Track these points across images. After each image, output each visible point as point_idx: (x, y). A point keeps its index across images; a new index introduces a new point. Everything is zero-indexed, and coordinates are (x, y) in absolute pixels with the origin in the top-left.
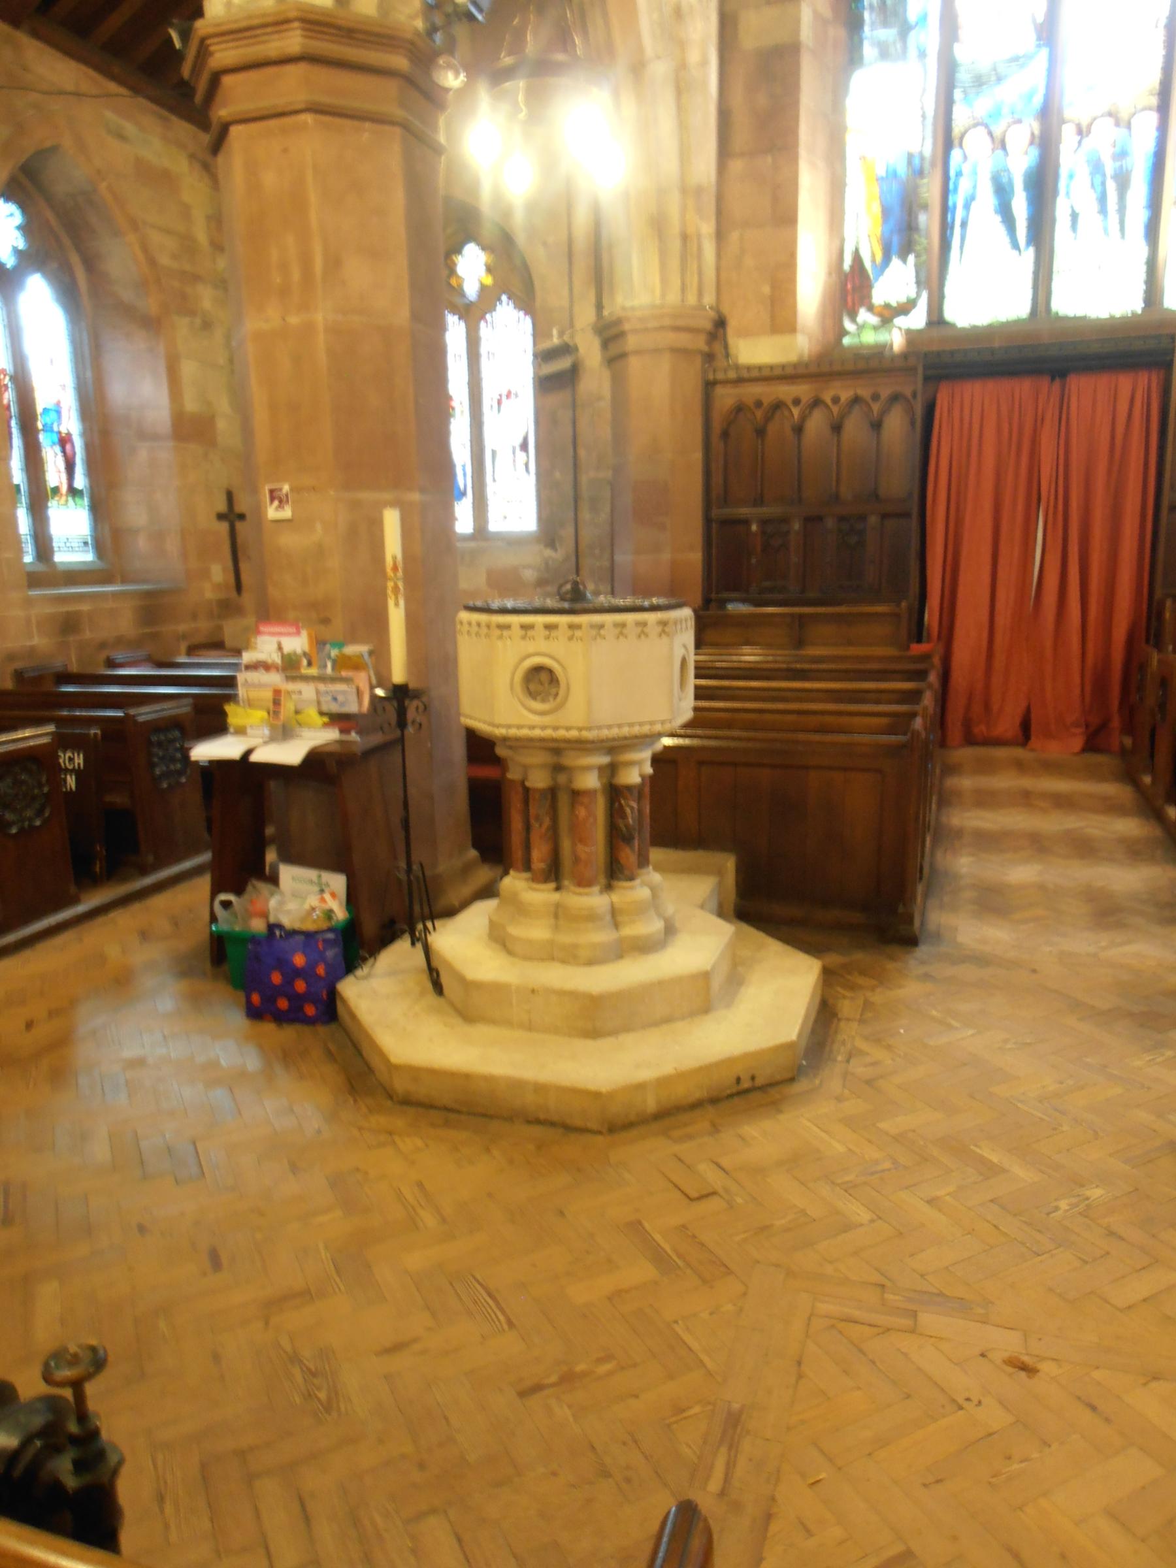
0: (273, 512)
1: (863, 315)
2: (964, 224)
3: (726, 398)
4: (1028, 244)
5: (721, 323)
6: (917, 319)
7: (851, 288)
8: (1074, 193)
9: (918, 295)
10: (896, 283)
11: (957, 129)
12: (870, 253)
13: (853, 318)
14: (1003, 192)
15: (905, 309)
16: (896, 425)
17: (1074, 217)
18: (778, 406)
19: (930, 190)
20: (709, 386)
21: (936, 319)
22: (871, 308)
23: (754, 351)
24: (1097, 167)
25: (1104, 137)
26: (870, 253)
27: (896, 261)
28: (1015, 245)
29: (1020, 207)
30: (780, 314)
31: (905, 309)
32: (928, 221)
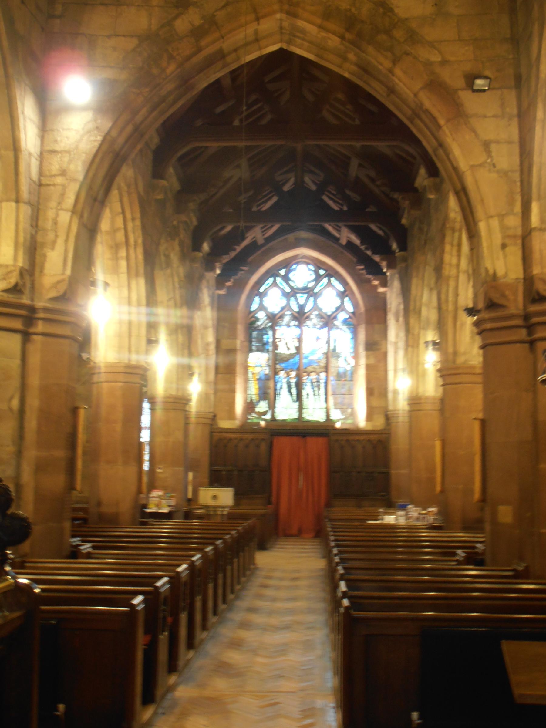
3: (217, 436)
5: (215, 416)
6: (268, 416)
7: (250, 406)
8: (307, 389)
10: (263, 406)
12: (255, 398)
14: (289, 387)
15: (265, 413)
16: (264, 447)
18: (231, 439)
19: (271, 384)
20: (212, 433)
21: (273, 419)
23: (224, 424)
25: (313, 376)
26: (255, 398)
29: (294, 391)
30: (231, 414)
31: (265, 413)
32: (271, 392)
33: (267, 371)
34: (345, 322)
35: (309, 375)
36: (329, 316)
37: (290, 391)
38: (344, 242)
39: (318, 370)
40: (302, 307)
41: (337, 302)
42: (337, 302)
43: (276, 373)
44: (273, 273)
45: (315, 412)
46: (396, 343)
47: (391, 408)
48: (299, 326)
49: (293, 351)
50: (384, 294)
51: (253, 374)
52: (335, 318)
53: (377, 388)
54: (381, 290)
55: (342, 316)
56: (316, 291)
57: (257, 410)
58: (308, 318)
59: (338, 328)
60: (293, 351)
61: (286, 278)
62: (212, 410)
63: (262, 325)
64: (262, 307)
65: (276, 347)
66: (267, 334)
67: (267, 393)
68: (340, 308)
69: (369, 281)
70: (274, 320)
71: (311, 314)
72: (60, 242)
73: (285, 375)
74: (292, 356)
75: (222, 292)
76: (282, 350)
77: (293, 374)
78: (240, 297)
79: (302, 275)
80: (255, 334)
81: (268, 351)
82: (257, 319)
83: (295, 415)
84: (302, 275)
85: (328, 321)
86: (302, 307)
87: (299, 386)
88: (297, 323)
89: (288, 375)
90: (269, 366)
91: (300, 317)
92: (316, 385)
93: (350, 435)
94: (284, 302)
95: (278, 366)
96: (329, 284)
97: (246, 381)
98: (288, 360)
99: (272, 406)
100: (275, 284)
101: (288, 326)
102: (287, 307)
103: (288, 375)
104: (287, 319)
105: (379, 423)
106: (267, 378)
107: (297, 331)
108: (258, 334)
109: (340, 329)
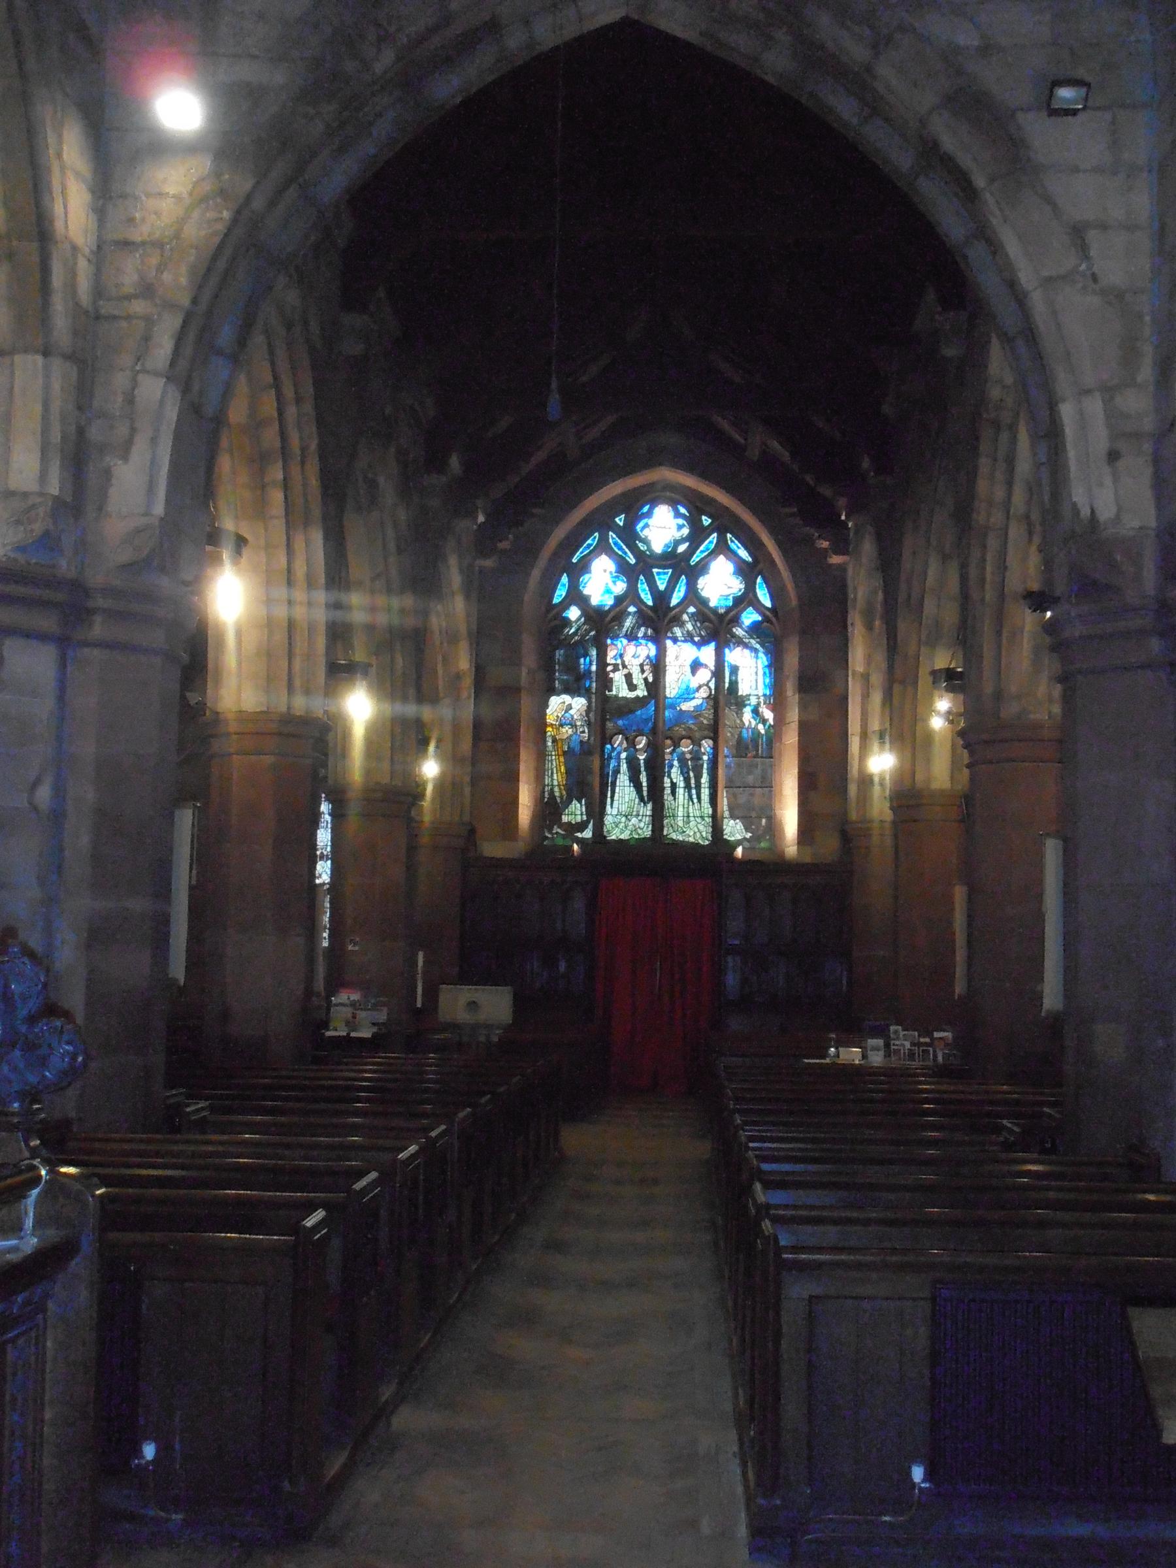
0: (350, 948)
1: (556, 829)
4: (649, 800)
5: (472, 831)
7: (548, 810)
9: (588, 822)
10: (576, 812)
11: (608, 733)
13: (550, 831)
17: (674, 786)
22: (561, 825)
23: (493, 849)
24: (683, 761)
25: (686, 748)
27: (574, 801)
28: (642, 799)
31: (582, 826)
34: (755, 629)
35: (676, 745)
36: (721, 617)
37: (635, 780)
38: (754, 454)
39: (697, 735)
40: (661, 598)
41: (736, 586)
42: (736, 586)
43: (605, 738)
44: (600, 521)
45: (689, 822)
46: (866, 677)
47: (853, 816)
48: (658, 638)
49: (641, 692)
50: (842, 568)
51: (554, 741)
52: (736, 621)
53: (825, 775)
54: (835, 560)
55: (750, 617)
56: (695, 559)
57: (565, 819)
58: (677, 621)
59: (740, 642)
60: (641, 692)
61: (630, 536)
62: (467, 818)
63: (575, 633)
64: (576, 596)
66: (585, 655)
67: (589, 784)
68: (746, 599)
69: (809, 541)
70: (603, 624)
71: (684, 611)
72: (140, 447)
73: (625, 745)
74: (640, 702)
75: (489, 563)
76: (620, 689)
77: (642, 742)
78: (528, 575)
79: (663, 527)
80: (559, 654)
81: (586, 693)
82: (567, 623)
83: (647, 832)
84: (663, 527)
85: (717, 628)
86: (661, 598)
87: (656, 769)
88: (650, 631)
89: (632, 744)
90: (589, 724)
91: (659, 621)
92: (691, 767)
93: (766, 872)
94: (621, 587)
95: (609, 725)
96: (722, 548)
97: (541, 756)
98: (632, 711)
99: (597, 813)
100: (603, 547)
101: (631, 637)
102: (632, 594)
103: (632, 744)
104: (629, 622)
105: (828, 847)
106: (586, 749)
107: (652, 650)
108: (566, 656)
109: (746, 646)
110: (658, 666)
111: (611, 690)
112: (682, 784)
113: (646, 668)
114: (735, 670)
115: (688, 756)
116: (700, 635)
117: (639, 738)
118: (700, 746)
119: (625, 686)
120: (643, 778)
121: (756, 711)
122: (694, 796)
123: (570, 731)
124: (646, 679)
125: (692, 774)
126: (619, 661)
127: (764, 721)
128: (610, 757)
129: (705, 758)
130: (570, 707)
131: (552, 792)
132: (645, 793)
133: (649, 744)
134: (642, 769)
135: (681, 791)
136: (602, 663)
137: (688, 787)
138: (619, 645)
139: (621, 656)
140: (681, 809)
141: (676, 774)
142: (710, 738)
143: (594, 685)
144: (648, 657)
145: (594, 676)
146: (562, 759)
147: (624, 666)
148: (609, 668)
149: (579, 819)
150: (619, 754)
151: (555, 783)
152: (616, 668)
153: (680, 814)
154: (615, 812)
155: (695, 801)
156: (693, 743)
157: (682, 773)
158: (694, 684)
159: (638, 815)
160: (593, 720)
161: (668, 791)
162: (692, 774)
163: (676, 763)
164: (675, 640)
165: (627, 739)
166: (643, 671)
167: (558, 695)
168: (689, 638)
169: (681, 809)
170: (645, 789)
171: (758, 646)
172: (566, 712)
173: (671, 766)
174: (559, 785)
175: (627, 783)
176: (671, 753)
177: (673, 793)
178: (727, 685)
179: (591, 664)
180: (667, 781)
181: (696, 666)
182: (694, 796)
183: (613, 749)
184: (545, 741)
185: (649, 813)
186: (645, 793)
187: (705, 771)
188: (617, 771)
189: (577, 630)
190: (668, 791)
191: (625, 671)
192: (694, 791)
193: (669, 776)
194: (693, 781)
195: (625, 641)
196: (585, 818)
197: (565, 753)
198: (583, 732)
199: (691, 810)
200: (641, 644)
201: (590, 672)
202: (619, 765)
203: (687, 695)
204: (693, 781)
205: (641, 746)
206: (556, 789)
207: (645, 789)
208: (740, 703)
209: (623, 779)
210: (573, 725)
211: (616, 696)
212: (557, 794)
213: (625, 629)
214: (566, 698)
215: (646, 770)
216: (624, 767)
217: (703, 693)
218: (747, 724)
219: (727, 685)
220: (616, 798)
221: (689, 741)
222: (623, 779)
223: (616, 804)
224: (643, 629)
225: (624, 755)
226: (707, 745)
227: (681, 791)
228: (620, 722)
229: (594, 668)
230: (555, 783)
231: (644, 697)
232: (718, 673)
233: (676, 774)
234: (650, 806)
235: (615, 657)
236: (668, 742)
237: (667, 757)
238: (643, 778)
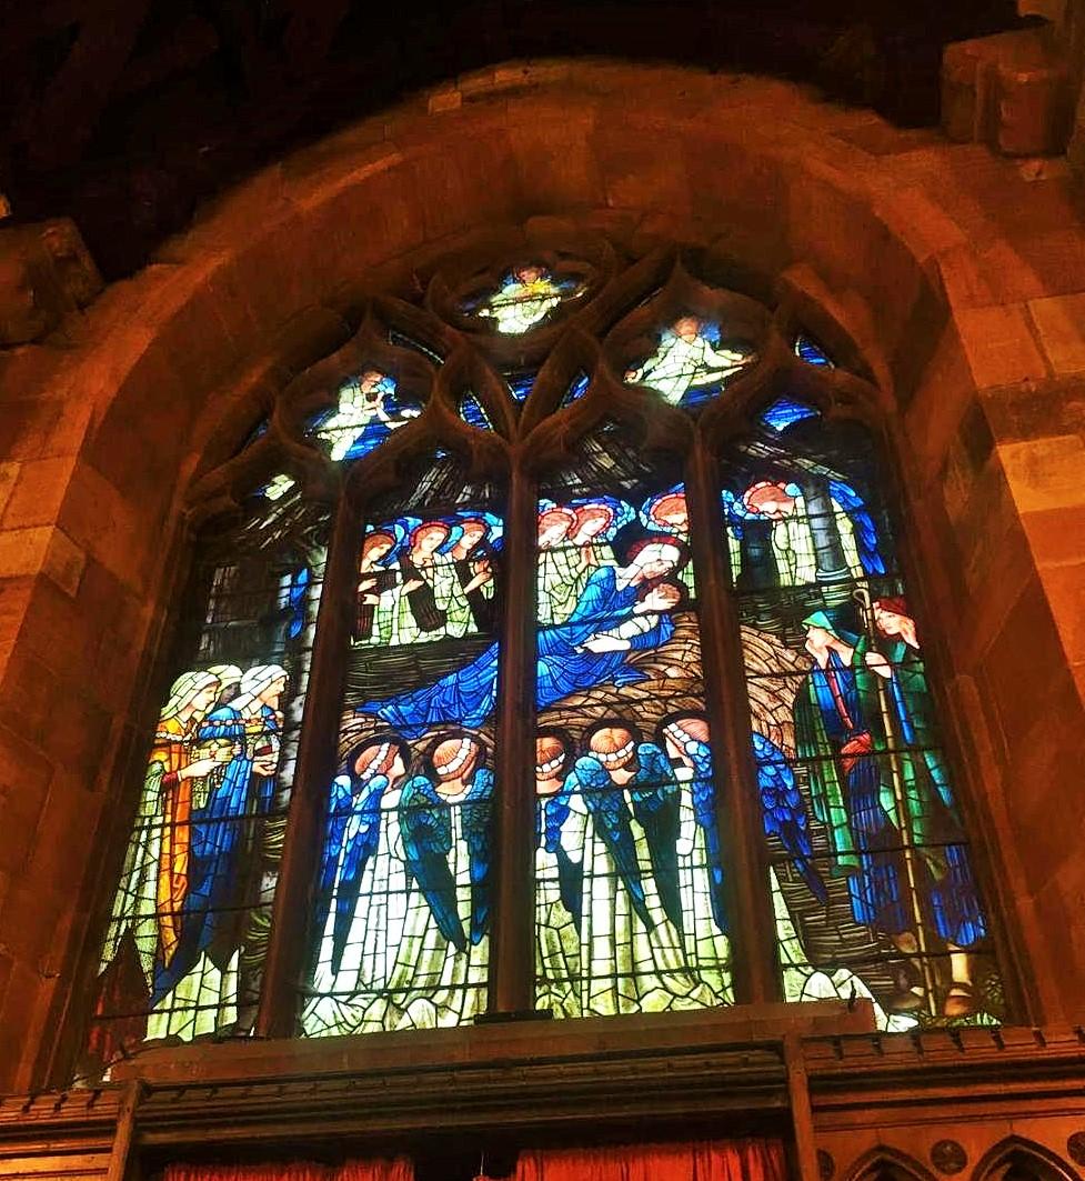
2: (350, 892)
11: (346, 743)
17: (572, 879)
24: (601, 791)
27: (204, 964)
28: (449, 930)
33: (276, 762)
35: (574, 747)
37: (430, 878)
39: (648, 712)
49: (460, 624)
51: (170, 785)
65: (349, 614)
73: (398, 767)
74: (458, 653)
76: (393, 621)
77: (456, 753)
87: (508, 827)
92: (637, 818)
95: (352, 721)
98: (428, 679)
99: (279, 988)
101: (440, 512)
110: (514, 562)
111: (369, 635)
112: (602, 865)
113: (476, 568)
114: (759, 531)
115: (621, 776)
116: (638, 474)
117: (448, 745)
118: (660, 740)
119: (409, 620)
120: (460, 860)
121: (847, 622)
122: (653, 902)
123: (222, 755)
124: (475, 597)
125: (637, 831)
126: (396, 566)
127: (885, 643)
128: (346, 811)
129: (684, 774)
130: (237, 691)
131: (130, 936)
132: (464, 910)
133: (480, 760)
134: (457, 832)
135: (600, 895)
136: (345, 574)
137: (625, 871)
138: (399, 531)
139: (403, 553)
140: (602, 948)
141: (575, 835)
142: (694, 714)
143: (312, 632)
144: (483, 543)
145: (315, 608)
146: (183, 835)
147: (410, 573)
148: (365, 585)
149: (207, 1024)
150: (378, 794)
151: (147, 908)
152: (384, 582)
153: (602, 967)
154: (346, 982)
155: (658, 916)
156: (636, 736)
157: (600, 829)
158: (627, 577)
159: (434, 987)
160: (298, 715)
161: (550, 893)
162: (637, 831)
163: (577, 803)
164: (563, 498)
165: (405, 753)
166: (465, 577)
167: (204, 665)
168: (604, 488)
169: (602, 948)
170: (463, 894)
171: (825, 470)
172: (219, 705)
173: (563, 813)
174: (157, 916)
175: (399, 882)
176: (560, 776)
177: (572, 898)
178: (736, 571)
179: (310, 584)
180: (545, 862)
181: (628, 543)
182: (653, 902)
183: (358, 784)
184: (141, 788)
185: (477, 976)
186: (464, 910)
187: (686, 816)
188: (367, 847)
189: (282, 518)
190: (550, 893)
191: (413, 585)
192: (649, 886)
193: (555, 846)
194: (643, 852)
195: (412, 522)
196: (231, 1015)
197: (195, 820)
198: (267, 750)
199: (642, 951)
200: (461, 521)
201: (305, 600)
202: (374, 829)
203: (611, 606)
204: (643, 852)
205: (453, 766)
206: (147, 928)
207: (463, 894)
208: (790, 612)
209: (387, 869)
210: (236, 737)
211: (383, 650)
212: (145, 945)
213: (414, 499)
214: (230, 673)
215: (468, 834)
216: (392, 833)
217: (657, 600)
218: (822, 661)
219: (736, 571)
220: (356, 931)
221: (618, 734)
222: (387, 869)
223: (351, 957)
224: (467, 489)
225: (391, 800)
226: (687, 739)
227: (600, 895)
228: (388, 710)
229: (316, 592)
230: (147, 908)
231: (467, 637)
232: (702, 545)
233: (575, 835)
234: (480, 953)
235: (384, 560)
236: (547, 743)
237: (543, 787)
238: (460, 860)
